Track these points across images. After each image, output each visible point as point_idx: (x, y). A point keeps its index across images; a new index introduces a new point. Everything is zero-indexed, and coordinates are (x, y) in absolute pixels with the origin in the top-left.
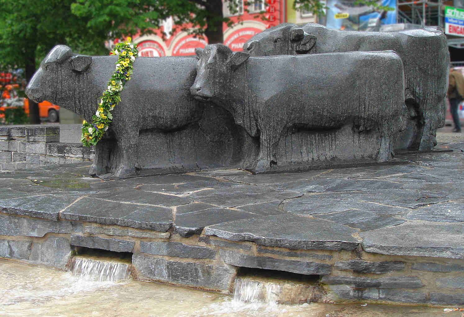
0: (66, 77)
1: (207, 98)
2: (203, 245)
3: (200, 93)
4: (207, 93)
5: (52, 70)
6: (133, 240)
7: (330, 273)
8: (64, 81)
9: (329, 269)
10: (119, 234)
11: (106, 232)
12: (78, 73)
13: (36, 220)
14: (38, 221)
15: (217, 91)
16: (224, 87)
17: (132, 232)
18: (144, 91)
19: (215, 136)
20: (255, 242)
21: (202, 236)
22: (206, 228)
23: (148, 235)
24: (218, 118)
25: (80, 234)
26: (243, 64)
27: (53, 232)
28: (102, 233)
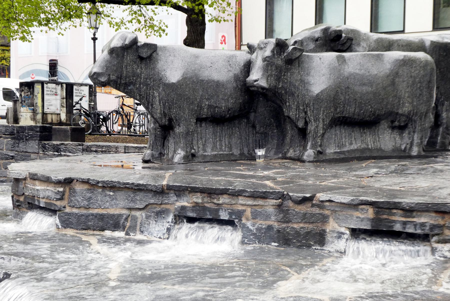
0: (131, 62)
1: (263, 88)
2: (316, 211)
3: (257, 84)
4: (263, 83)
5: (118, 56)
6: (244, 208)
7: (442, 232)
8: (129, 66)
9: (441, 228)
10: (228, 202)
11: (215, 201)
12: (142, 59)
13: (136, 192)
14: (138, 193)
15: (273, 83)
16: (278, 79)
17: (241, 200)
18: (202, 81)
19: (261, 127)
20: (372, 205)
21: (314, 202)
22: (318, 195)
23: (261, 202)
24: (265, 110)
25: (186, 204)
26: (300, 56)
27: (155, 203)
28: (210, 203)
